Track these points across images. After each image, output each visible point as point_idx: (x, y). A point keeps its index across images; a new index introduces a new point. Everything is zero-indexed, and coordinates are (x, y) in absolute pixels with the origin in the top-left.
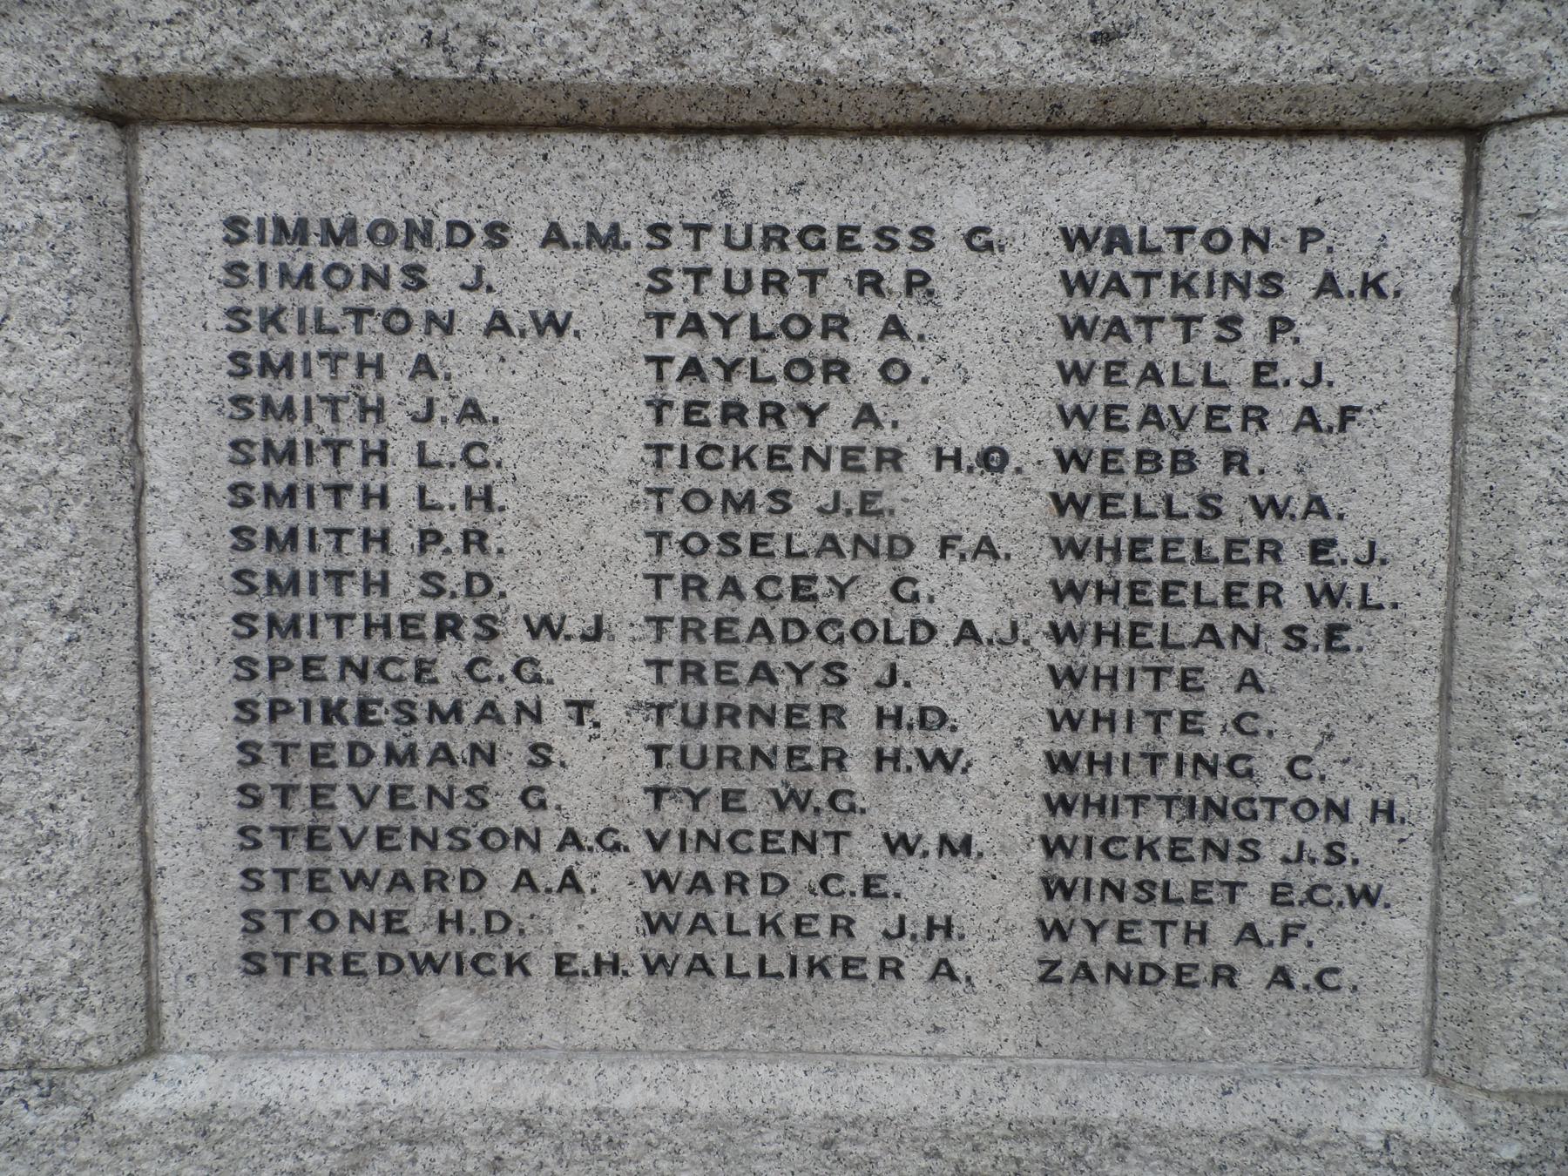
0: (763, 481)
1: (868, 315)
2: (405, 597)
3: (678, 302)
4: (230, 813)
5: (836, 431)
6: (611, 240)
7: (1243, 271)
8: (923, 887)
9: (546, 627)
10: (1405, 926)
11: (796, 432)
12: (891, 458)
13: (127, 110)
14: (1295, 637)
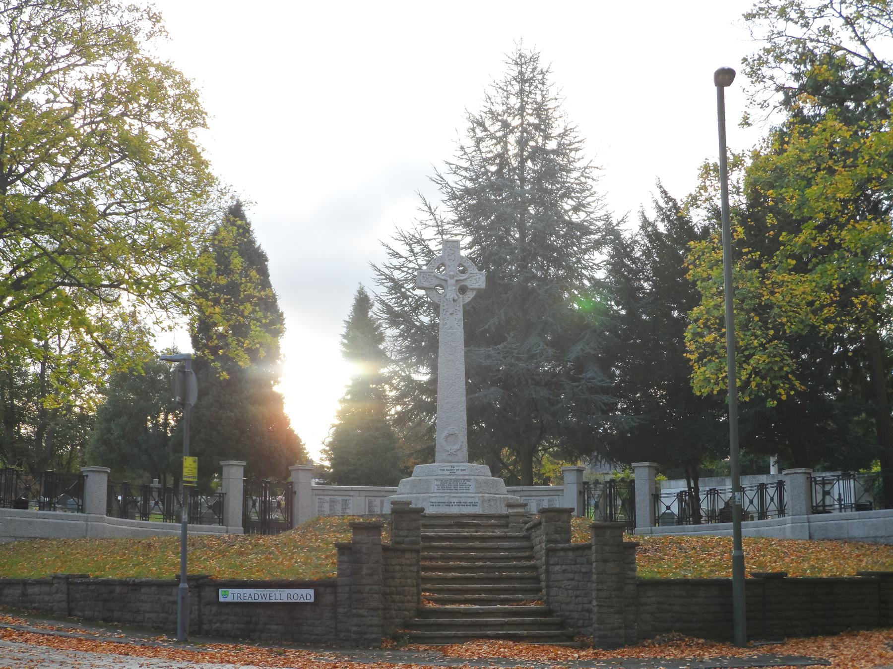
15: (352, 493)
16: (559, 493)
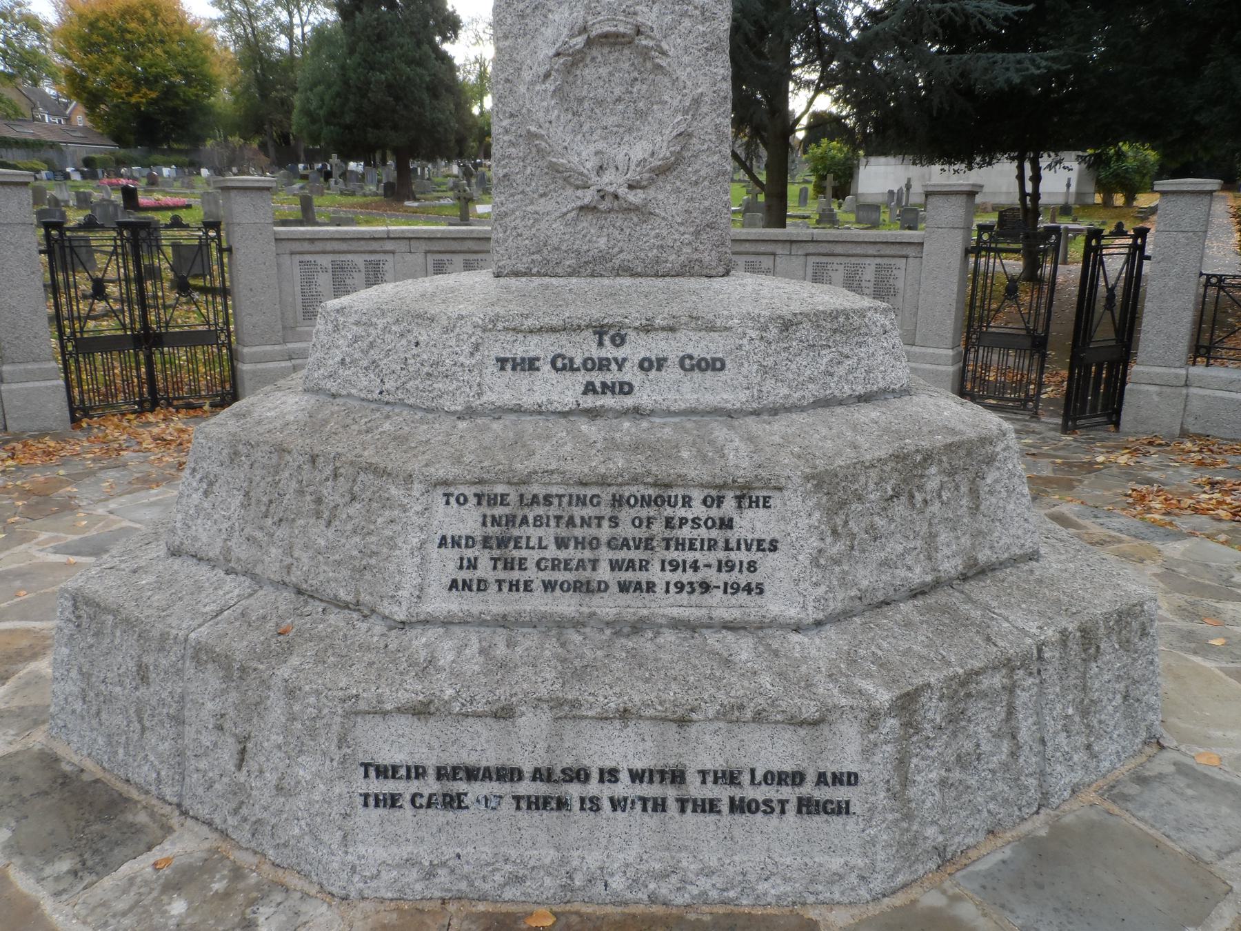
7: (889, 267)
13: (807, 255)
15: (389, 246)
16: (910, 251)
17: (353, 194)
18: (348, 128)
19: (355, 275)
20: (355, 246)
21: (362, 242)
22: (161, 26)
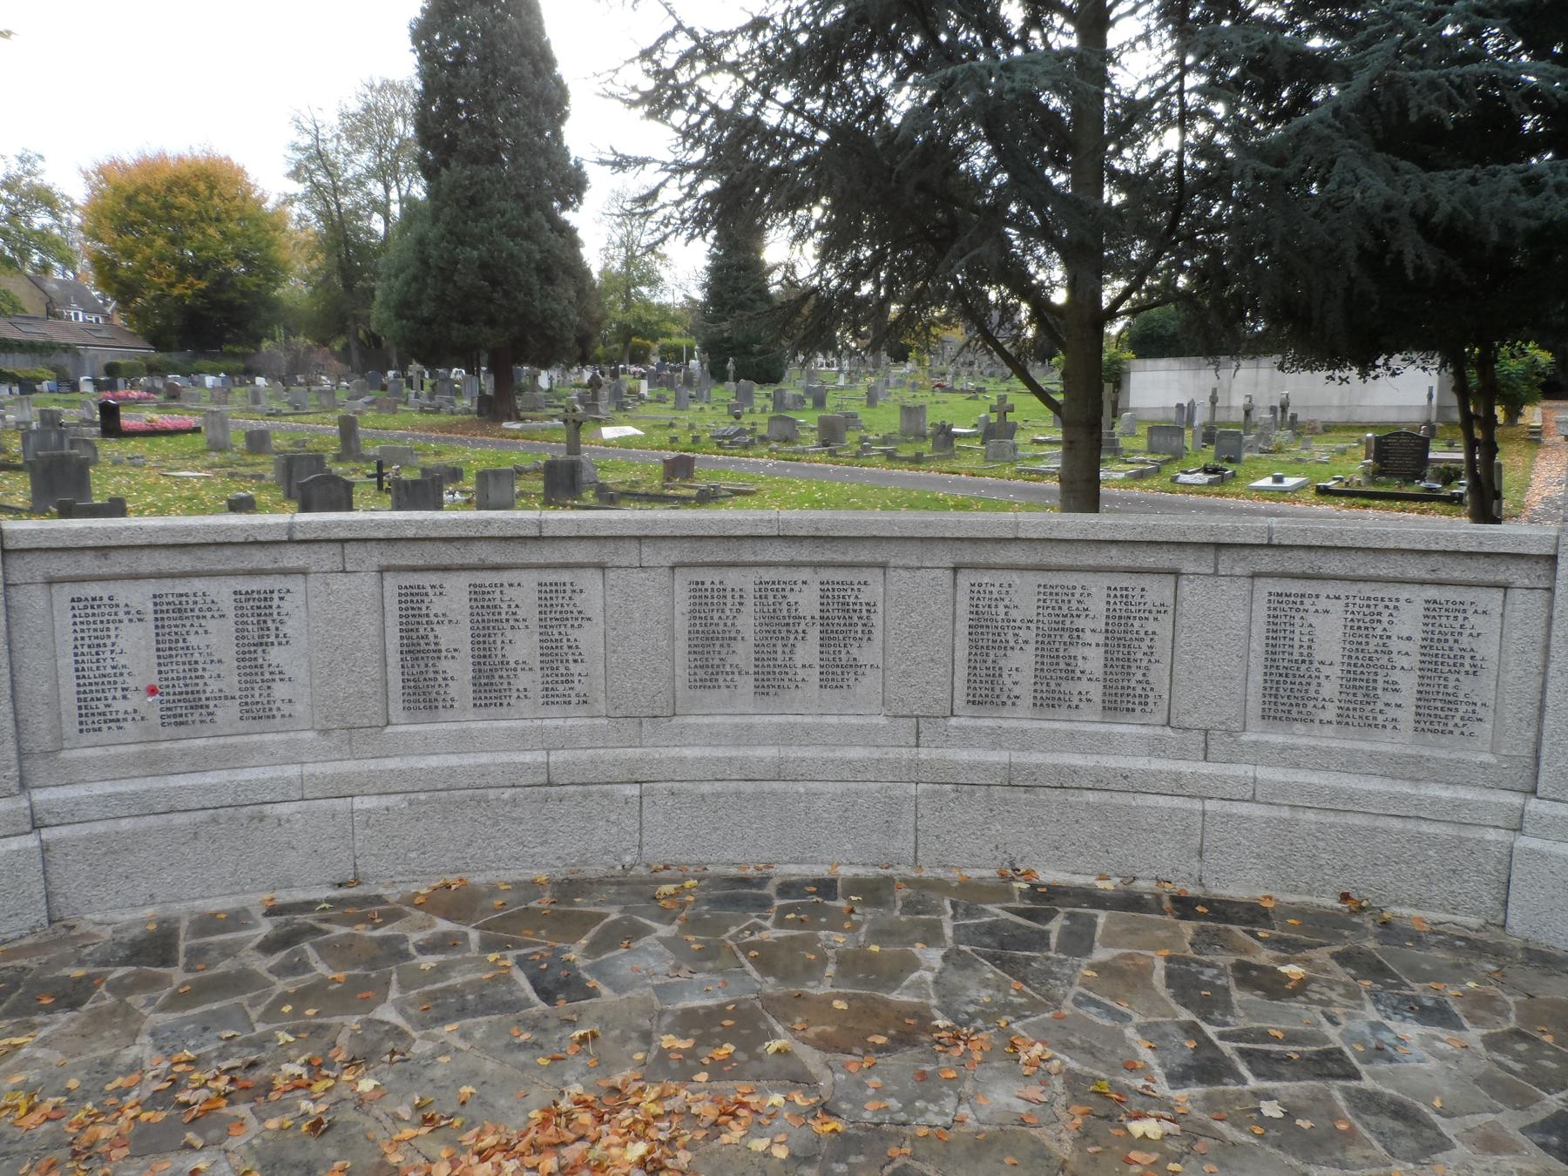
0: (1364, 640)
1: (1386, 613)
2: (1296, 656)
3: (1350, 608)
4: (1261, 691)
5: (1379, 632)
6: (1338, 598)
7: (1459, 608)
8: (1391, 713)
9: (1322, 663)
10: (1488, 726)
11: (1371, 632)
12: (1389, 637)
13: (1254, 576)
14: (1467, 673)
15: (293, 558)
17: (437, 410)
18: (427, 322)
19: (210, 624)
20: (210, 560)
21: (228, 552)
22: (216, 201)
